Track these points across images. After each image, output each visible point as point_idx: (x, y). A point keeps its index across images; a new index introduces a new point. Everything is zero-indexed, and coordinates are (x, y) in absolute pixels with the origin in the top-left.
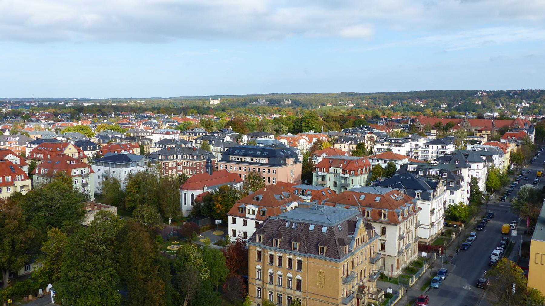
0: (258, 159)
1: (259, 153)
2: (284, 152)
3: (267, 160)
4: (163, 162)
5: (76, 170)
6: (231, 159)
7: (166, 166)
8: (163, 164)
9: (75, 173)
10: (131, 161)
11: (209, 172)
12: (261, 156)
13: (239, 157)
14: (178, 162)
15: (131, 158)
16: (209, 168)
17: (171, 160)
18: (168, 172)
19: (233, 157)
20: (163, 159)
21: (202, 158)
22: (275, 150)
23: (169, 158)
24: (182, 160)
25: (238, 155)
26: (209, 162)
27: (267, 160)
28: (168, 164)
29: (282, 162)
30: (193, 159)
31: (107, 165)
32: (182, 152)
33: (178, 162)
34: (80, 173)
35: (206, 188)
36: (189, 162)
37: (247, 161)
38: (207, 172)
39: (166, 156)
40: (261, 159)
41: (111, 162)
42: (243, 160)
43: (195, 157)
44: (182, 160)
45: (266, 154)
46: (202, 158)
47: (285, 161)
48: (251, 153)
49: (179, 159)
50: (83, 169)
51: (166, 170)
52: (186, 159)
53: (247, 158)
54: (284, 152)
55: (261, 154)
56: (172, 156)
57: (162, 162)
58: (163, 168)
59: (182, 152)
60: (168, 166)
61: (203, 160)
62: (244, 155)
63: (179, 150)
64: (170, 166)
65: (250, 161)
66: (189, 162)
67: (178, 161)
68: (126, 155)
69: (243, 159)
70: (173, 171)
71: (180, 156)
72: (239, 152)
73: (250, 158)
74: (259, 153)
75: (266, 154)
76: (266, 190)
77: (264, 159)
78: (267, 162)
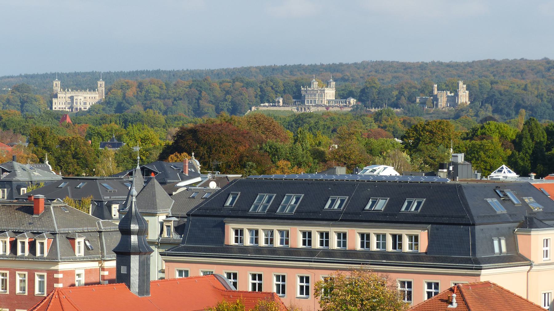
0: (373, 233)
2: (506, 200)
6: (231, 239)
19: (246, 227)
21: (80, 251)
22: (460, 187)
27: (423, 237)
29: (497, 250)
40: (389, 232)
42: (298, 242)
46: (80, 251)
47: (512, 245)
54: (506, 200)
55: (388, 206)
61: (81, 260)
76: (455, 305)
77: (405, 233)
78: (423, 246)
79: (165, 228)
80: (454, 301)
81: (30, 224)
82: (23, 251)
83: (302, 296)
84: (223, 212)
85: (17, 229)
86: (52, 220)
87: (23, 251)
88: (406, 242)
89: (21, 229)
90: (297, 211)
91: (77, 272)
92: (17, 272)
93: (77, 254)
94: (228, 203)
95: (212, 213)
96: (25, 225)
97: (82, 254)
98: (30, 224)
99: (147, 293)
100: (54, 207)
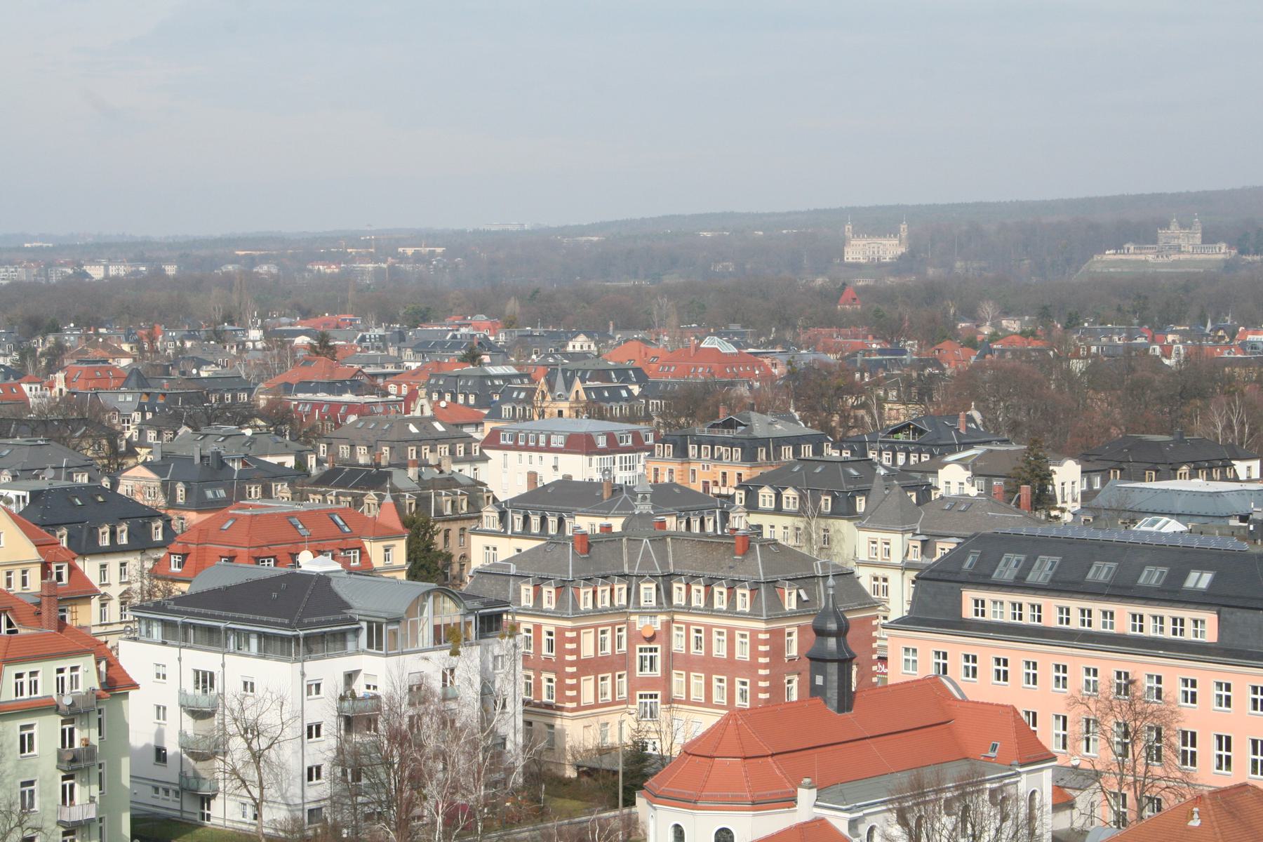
0: (1147, 611)
1: (1152, 576)
3: (1210, 619)
4: (549, 625)
5: (26, 669)
6: (968, 612)
7: (562, 652)
8: (545, 637)
9: (19, 689)
10: (352, 621)
11: (833, 694)
12: (1171, 594)
13: (1026, 600)
14: (639, 627)
15: (351, 602)
16: (833, 668)
17: (597, 612)
18: (577, 687)
19: (988, 596)
20: (546, 605)
23: (586, 603)
24: (664, 617)
25: (1019, 585)
26: (833, 626)
28: (577, 640)
30: (732, 612)
31: (212, 638)
32: (664, 562)
33: (639, 627)
34: (47, 687)
35: (806, 796)
36: (709, 629)
37: (1075, 624)
38: (815, 691)
39: (561, 587)
40: (1168, 613)
41: (233, 620)
42: (1051, 619)
43: (743, 599)
44: (664, 617)
45: (1200, 580)
48: (1101, 572)
49: (642, 614)
50: (67, 664)
51: (561, 676)
52: (688, 609)
53: (1075, 605)
56: (603, 591)
57: (538, 628)
58: (547, 665)
59: (664, 562)
60: (577, 652)
62: (1056, 588)
63: (646, 552)
64: (588, 650)
65: (1097, 626)
66: (709, 629)
67: (641, 623)
68: (323, 580)
69: (1051, 611)
70: (609, 681)
71: (648, 591)
72: (1027, 567)
73: (1097, 607)
74: (1152, 576)
75: (1200, 580)
77: (1188, 615)
78: (1210, 634)
79: (911, 550)
80: (1196, 816)
81: (731, 567)
82: (720, 602)
83: (1058, 689)
84: (962, 578)
85: (714, 574)
86: (758, 564)
87: (720, 602)
88: (1189, 626)
89: (720, 574)
90: (1051, 580)
91: (787, 630)
92: (714, 630)
93: (787, 608)
94: (966, 566)
95: (946, 577)
96: (725, 569)
97: (794, 606)
98: (731, 567)
99: (849, 709)
100: (761, 546)
